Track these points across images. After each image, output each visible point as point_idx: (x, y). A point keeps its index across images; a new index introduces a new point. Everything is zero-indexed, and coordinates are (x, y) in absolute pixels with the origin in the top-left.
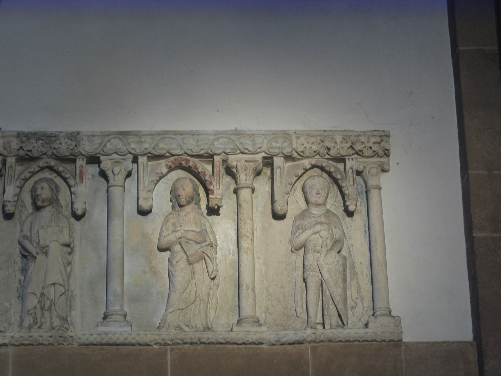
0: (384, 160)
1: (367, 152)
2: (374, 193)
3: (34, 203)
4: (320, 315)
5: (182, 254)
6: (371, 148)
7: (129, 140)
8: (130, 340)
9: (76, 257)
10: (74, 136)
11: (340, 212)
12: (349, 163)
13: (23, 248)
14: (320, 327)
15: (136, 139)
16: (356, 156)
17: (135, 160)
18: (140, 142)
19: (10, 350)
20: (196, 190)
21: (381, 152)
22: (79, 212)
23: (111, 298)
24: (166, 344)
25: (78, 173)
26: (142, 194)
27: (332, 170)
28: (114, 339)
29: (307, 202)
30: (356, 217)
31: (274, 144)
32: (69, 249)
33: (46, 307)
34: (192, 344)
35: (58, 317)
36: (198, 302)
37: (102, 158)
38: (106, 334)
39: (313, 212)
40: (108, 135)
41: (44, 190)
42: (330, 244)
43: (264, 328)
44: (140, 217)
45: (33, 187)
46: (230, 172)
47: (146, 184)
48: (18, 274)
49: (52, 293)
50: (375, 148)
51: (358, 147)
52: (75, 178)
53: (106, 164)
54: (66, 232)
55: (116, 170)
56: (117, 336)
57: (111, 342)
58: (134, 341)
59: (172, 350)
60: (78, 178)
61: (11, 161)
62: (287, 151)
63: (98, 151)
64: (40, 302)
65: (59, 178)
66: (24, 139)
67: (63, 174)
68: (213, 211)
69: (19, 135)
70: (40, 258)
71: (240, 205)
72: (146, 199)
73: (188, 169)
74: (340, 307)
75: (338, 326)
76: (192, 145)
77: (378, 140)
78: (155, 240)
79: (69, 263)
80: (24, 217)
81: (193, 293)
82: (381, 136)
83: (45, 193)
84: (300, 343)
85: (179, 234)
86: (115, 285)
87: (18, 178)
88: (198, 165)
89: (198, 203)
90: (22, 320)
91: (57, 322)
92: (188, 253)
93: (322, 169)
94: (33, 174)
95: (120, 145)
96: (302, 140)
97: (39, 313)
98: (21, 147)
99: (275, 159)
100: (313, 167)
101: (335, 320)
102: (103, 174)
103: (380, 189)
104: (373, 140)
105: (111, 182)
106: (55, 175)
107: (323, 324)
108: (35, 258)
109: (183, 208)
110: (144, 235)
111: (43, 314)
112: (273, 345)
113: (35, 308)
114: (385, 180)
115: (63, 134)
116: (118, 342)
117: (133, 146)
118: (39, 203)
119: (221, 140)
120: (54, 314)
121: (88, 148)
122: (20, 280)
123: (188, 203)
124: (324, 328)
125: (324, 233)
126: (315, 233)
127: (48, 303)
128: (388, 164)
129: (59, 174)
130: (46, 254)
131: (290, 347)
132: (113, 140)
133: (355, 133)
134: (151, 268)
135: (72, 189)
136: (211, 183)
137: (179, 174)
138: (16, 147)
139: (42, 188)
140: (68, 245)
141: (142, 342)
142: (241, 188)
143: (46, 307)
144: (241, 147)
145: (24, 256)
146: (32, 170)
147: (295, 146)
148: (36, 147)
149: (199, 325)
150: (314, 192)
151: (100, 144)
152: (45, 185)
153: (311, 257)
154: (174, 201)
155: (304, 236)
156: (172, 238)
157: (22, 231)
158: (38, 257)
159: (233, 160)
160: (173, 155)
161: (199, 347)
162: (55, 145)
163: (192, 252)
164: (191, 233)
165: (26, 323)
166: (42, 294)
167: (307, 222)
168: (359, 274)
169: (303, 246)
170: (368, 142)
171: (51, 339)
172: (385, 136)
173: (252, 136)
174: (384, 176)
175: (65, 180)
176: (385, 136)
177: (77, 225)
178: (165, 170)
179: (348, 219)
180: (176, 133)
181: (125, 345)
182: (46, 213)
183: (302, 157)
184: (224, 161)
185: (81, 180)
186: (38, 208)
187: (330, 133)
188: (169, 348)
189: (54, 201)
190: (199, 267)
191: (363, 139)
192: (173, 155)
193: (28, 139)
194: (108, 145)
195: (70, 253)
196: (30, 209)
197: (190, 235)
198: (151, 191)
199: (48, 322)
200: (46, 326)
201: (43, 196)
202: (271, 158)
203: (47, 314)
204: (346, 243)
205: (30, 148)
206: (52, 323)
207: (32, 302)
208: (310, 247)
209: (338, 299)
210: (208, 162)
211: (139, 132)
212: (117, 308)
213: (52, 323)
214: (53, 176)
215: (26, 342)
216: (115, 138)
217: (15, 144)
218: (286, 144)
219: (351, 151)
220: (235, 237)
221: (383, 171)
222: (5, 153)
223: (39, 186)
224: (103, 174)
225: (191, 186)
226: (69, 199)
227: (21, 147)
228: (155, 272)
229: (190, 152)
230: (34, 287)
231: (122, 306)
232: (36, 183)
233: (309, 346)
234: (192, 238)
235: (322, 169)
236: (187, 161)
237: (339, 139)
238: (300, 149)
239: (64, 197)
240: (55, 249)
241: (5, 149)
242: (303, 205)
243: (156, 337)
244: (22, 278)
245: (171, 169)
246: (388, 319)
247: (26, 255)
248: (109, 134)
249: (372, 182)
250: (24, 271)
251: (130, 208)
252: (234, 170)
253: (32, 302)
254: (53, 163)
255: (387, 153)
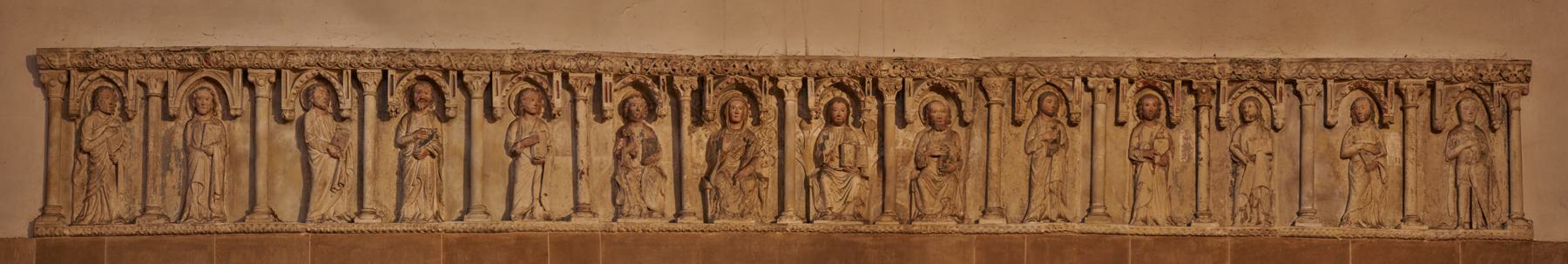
0: (1524, 85)
1: (1511, 79)
2: (1515, 114)
3: (1242, 117)
4: (1468, 215)
5: (1361, 163)
6: (1515, 75)
7: (1321, 67)
8: (1321, 234)
9: (1275, 163)
10: (1276, 62)
11: (1485, 127)
12: (1496, 88)
13: (1234, 155)
14: (1467, 226)
15: (1326, 66)
16: (1503, 81)
17: (1325, 83)
18: (1329, 68)
19: (1228, 239)
20: (1372, 108)
21: (1523, 79)
22: (1279, 126)
23: (1304, 198)
24: (1349, 238)
25: (1278, 93)
26: (1330, 112)
27: (1482, 93)
28: (1309, 233)
29: (1460, 118)
30: (1498, 133)
31: (1438, 71)
32: (1271, 157)
33: (1255, 205)
34: (1368, 238)
35: (1264, 213)
36: (1373, 203)
37: (1298, 81)
38: (1303, 228)
39: (1466, 129)
40: (1303, 62)
41: (1251, 109)
42: (1478, 156)
43: (1426, 227)
44: (1326, 130)
45: (1241, 104)
46: (1398, 92)
47: (1333, 104)
48: (1230, 176)
49: (1259, 194)
50: (1518, 75)
51: (1505, 74)
52: (1275, 97)
53: (1301, 86)
54: (1269, 143)
55: (1310, 91)
56: (1312, 230)
57: (1306, 235)
58: (1324, 235)
59: (1353, 242)
60: (1278, 97)
61: (1224, 83)
62: (1448, 77)
63: (1296, 75)
64: (1249, 201)
65: (1261, 96)
66: (1236, 65)
67: (1266, 94)
68: (1383, 126)
69: (1232, 61)
70: (1250, 165)
71: (1407, 122)
72: (1333, 116)
73: (1366, 90)
74: (1485, 211)
75: (1483, 226)
76: (1371, 70)
77: (1522, 68)
78: (1338, 150)
79: (1270, 169)
80: (1233, 129)
81: (1370, 195)
82: (1525, 65)
83: (1251, 109)
84: (1453, 239)
85: (1359, 146)
86: (1307, 188)
87: (1229, 97)
88: (1375, 87)
89: (1373, 120)
90: (1234, 216)
91: (1262, 218)
92: (1367, 163)
93: (1473, 91)
94: (1241, 93)
95: (1313, 71)
96: (1461, 67)
97: (1248, 210)
98: (1233, 72)
99: (1437, 83)
100: (1467, 89)
101: (1481, 220)
102: (1297, 94)
103: (1519, 110)
104: (1518, 69)
105: (1305, 101)
106: (1258, 94)
107: (1471, 224)
108: (1246, 165)
109: (1361, 124)
110: (1329, 145)
111: (1252, 211)
112: (1432, 240)
113: (1246, 206)
114: (1524, 102)
115: (1266, 61)
116: (1312, 235)
117: (1324, 71)
118: (1248, 119)
119: (1395, 67)
120: (1261, 211)
121: (1287, 72)
122: (1231, 181)
123: (1366, 120)
124: (1471, 227)
125: (1475, 148)
126: (1467, 148)
127: (1256, 202)
128: (1528, 90)
129: (1262, 93)
130: (1254, 161)
131: (1445, 242)
132: (1307, 67)
133: (1504, 62)
134: (1335, 173)
135: (1274, 107)
136: (1385, 103)
137: (1358, 93)
138: (1229, 72)
139: (1250, 106)
140: (1270, 154)
141: (1330, 235)
142: (1409, 107)
143: (1255, 205)
144: (1410, 72)
145: (1234, 162)
146: (1241, 91)
147: (1454, 72)
148: (1245, 71)
149: (1374, 222)
150: (1468, 112)
151: (1297, 70)
152: (1252, 103)
153: (1463, 168)
154: (1354, 117)
155: (1458, 149)
156: (1353, 149)
157: (1232, 141)
158: (1249, 165)
159: (1404, 83)
160: (1355, 79)
161: (1374, 241)
162: (1261, 70)
163: (1370, 162)
164: (1369, 146)
165: (1238, 218)
166: (1251, 195)
167: (1459, 137)
168: (1499, 182)
169: (1457, 158)
170: (1514, 70)
171: (1259, 232)
172: (1528, 65)
173: (1420, 63)
174: (1523, 99)
175: (1267, 98)
176: (1528, 65)
177: (1276, 136)
178: (1348, 91)
179: (1491, 134)
180: (1358, 60)
181: (1316, 237)
182: (1251, 129)
183: (1460, 80)
184: (1397, 84)
185: (1281, 100)
186: (1245, 122)
187: (1482, 62)
188: (1350, 241)
189: (1258, 117)
190: (1374, 174)
191: (1510, 67)
192: (1355, 79)
193: (1239, 65)
194: (1304, 71)
195: (1271, 160)
196: (1239, 123)
197: (1368, 148)
198: (1337, 109)
199: (1256, 218)
200: (1254, 221)
201: (1251, 113)
202: (1434, 82)
203: (1254, 210)
204: (1490, 154)
205: (1240, 72)
206: (1258, 219)
207: (1242, 201)
208: (1463, 158)
209: (1484, 205)
210: (1382, 84)
211: (1328, 59)
212: (1310, 207)
213: (1258, 219)
214: (1256, 95)
215: (1241, 234)
216: (1309, 64)
217: (1228, 68)
218: (1448, 71)
219: (1499, 77)
220: (1400, 147)
221: (1523, 94)
222: (1220, 76)
223: (1246, 104)
224: (1297, 94)
225: (1369, 105)
226: (1269, 114)
227: (1233, 72)
228: (1338, 177)
229: (1369, 77)
230: (1243, 188)
231: (1313, 206)
232: (1244, 101)
233: (1460, 242)
234: (1369, 150)
235: (1473, 91)
236: (1366, 84)
237: (1490, 67)
238: (1459, 75)
239: (1266, 111)
240: (1261, 157)
241: (1220, 73)
242: (1456, 122)
243: (1341, 232)
244: (1233, 180)
245: (1352, 90)
246: (1522, 223)
247: (1236, 161)
248: (1304, 61)
249: (1514, 104)
250: (1234, 173)
251: (1319, 121)
252: (1403, 91)
253: (1242, 201)
254: (1258, 85)
255: (1528, 79)
